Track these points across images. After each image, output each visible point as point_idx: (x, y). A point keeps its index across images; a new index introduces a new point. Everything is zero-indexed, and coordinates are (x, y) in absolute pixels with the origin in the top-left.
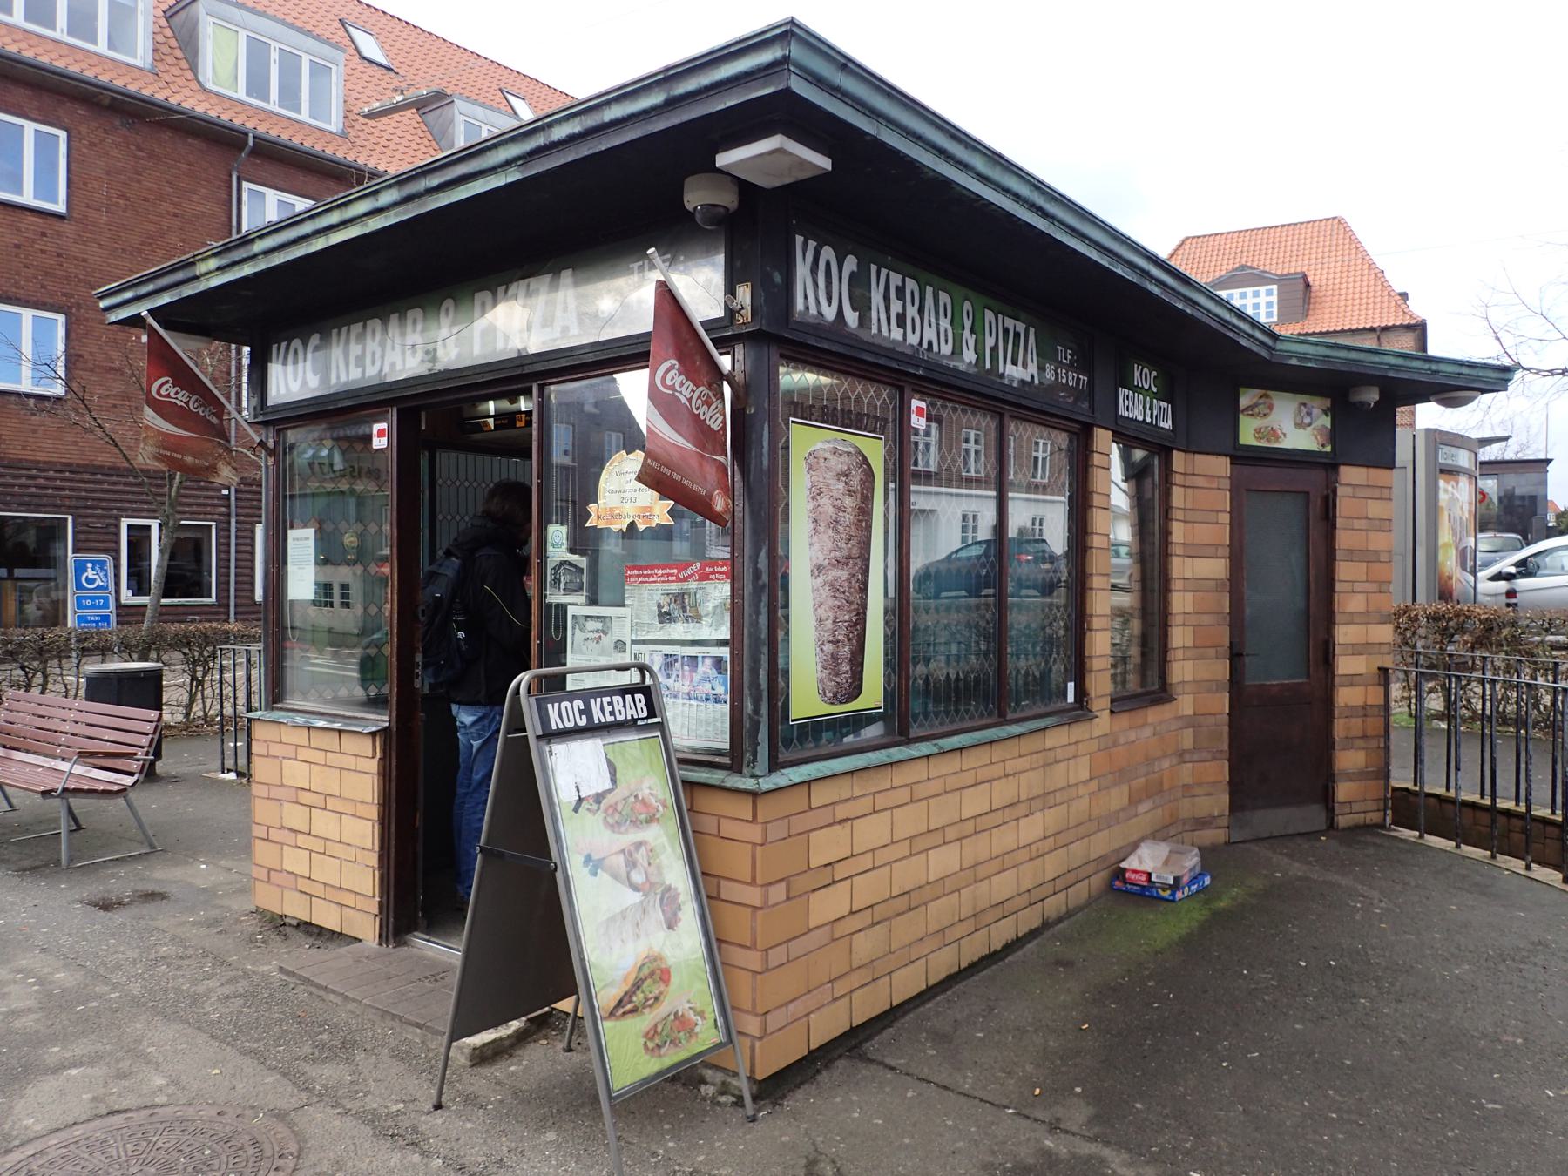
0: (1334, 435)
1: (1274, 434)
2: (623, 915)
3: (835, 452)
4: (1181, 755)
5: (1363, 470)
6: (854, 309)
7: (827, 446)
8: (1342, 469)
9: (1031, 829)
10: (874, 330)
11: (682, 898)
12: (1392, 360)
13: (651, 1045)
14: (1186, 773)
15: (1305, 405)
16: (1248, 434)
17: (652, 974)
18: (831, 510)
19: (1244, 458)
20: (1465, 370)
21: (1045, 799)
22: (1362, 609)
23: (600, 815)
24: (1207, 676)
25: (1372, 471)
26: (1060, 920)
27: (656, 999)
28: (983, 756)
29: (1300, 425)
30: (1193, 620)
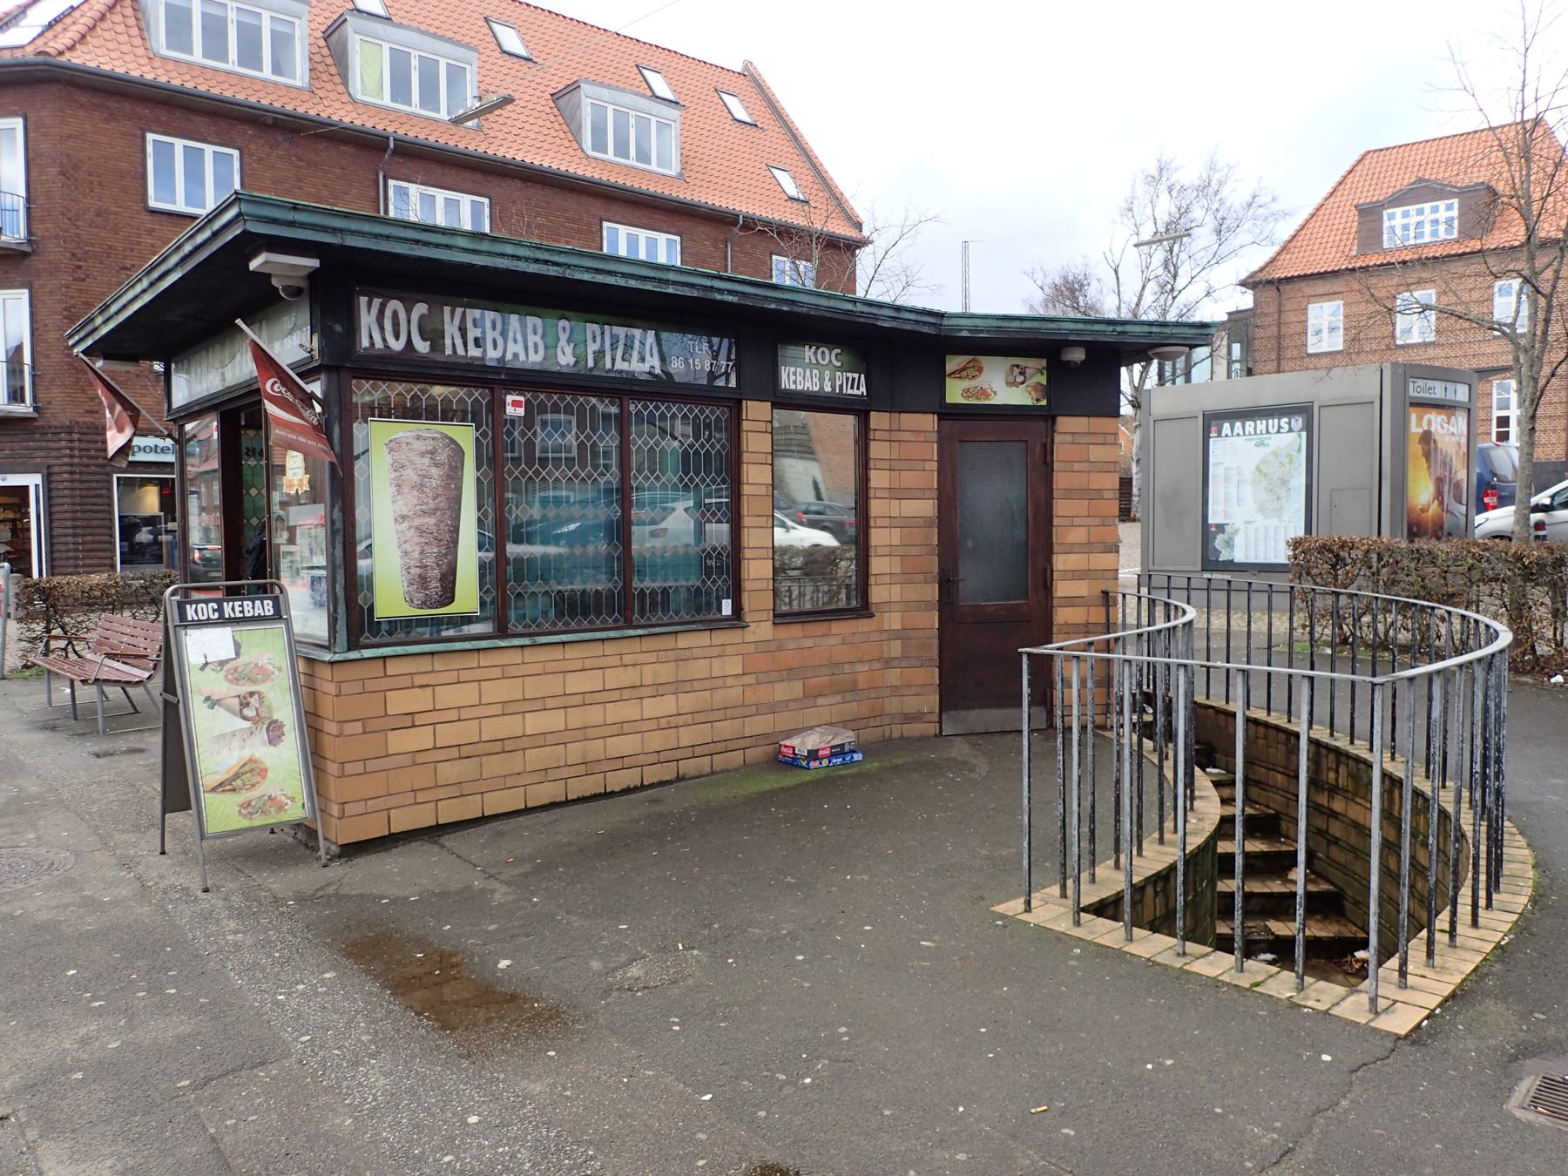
0: (1048, 391)
1: (984, 392)
2: (233, 734)
3: (418, 438)
4: (888, 663)
5: (1085, 420)
6: (424, 339)
7: (409, 434)
8: (1060, 420)
9: (666, 705)
10: (449, 351)
11: (285, 730)
12: (1071, 326)
13: (244, 811)
14: (894, 676)
15: (1018, 366)
16: (955, 393)
17: (252, 770)
18: (415, 478)
19: (949, 414)
20: (1155, 329)
21: (679, 686)
22: (1084, 540)
23: (222, 674)
24: (915, 597)
25: (1092, 420)
26: (691, 778)
27: (253, 785)
28: (597, 649)
29: (1013, 384)
30: (902, 551)
